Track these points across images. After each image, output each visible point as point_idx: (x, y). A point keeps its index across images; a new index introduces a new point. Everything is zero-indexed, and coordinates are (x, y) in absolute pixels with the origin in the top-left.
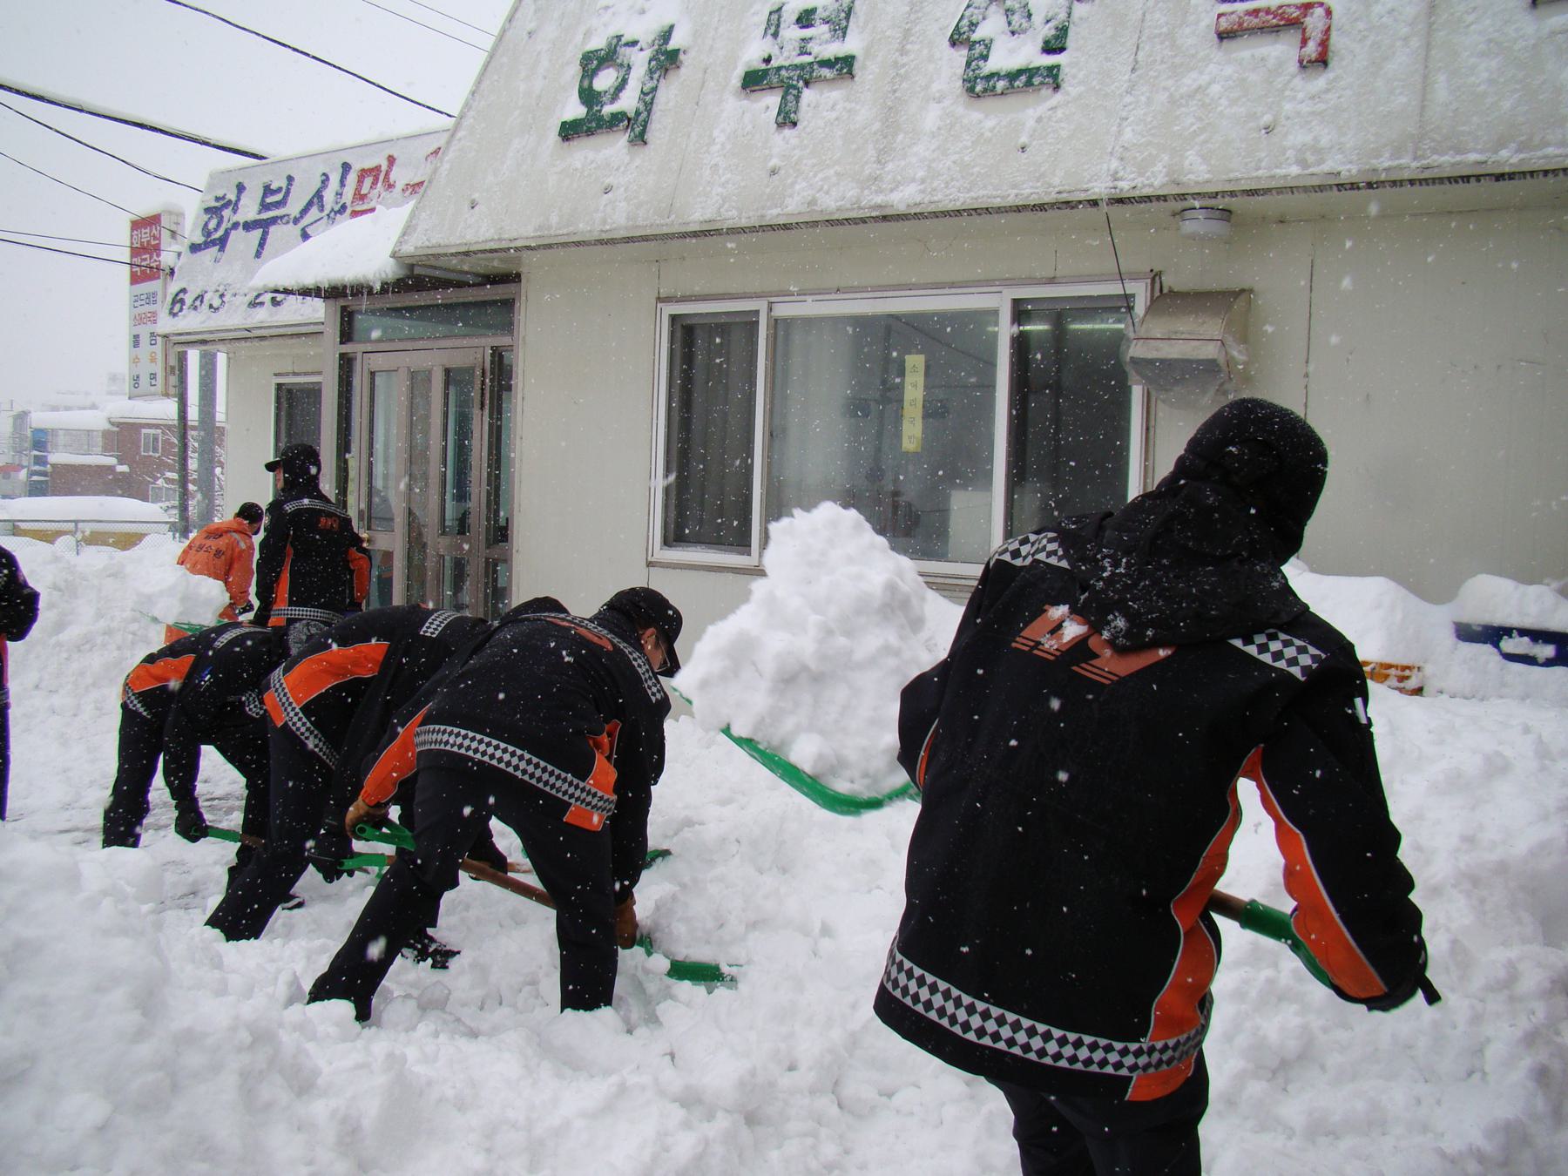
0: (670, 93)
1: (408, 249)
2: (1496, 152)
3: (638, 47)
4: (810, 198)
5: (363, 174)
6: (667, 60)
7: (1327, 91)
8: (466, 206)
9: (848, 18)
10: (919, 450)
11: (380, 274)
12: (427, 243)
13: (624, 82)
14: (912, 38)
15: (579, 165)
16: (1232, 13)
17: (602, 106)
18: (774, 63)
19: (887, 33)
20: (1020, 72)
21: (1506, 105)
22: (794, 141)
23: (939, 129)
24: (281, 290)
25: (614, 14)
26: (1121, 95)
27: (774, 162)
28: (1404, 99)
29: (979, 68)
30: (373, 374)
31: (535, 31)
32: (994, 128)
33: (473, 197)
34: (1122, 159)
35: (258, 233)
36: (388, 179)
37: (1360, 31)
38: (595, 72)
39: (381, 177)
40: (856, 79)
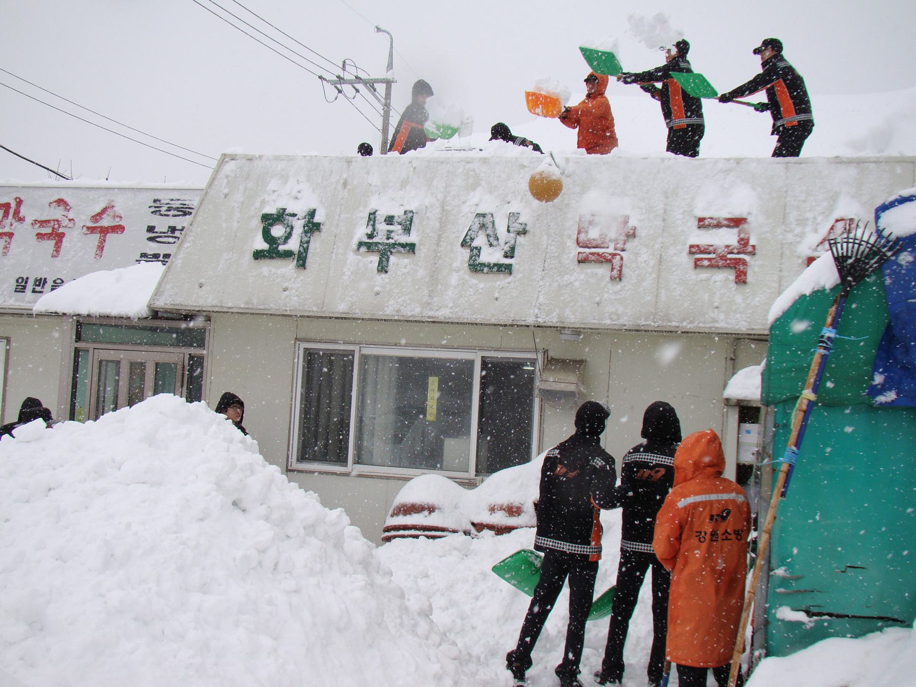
1: (160, 303)
2: (682, 323)
3: (297, 217)
4: (397, 309)
6: (312, 227)
7: (621, 291)
8: (197, 287)
9: (411, 224)
10: (435, 420)
11: (138, 315)
12: (172, 302)
13: (288, 236)
14: (442, 240)
15: (267, 275)
16: (585, 252)
17: (278, 246)
18: (375, 240)
19: (430, 235)
20: (495, 265)
21: (686, 305)
22: (387, 280)
23: (458, 285)
24: (61, 314)
25: (278, 195)
26: (538, 281)
27: (377, 289)
28: (649, 298)
29: (476, 260)
30: (101, 362)
31: (228, 194)
32: (484, 288)
33: (201, 281)
34: (539, 309)
36: (19, 212)
37: (633, 268)
38: (272, 225)
39: (12, 211)
40: (416, 254)
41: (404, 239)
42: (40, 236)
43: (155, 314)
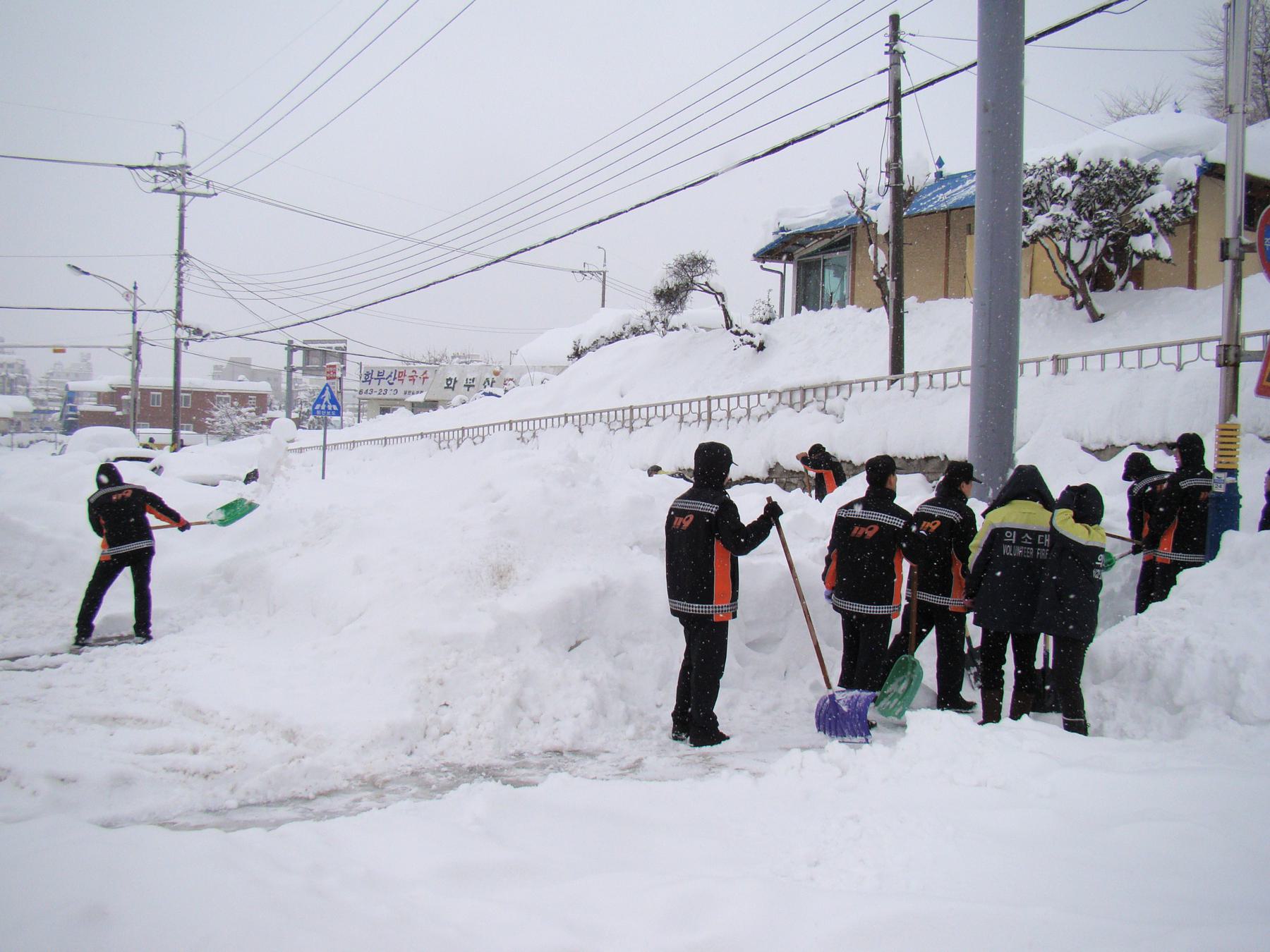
0: (456, 385)
5: (400, 372)
6: (455, 381)
35: (378, 380)
41: (472, 384)
42: (410, 380)
43: (426, 401)
